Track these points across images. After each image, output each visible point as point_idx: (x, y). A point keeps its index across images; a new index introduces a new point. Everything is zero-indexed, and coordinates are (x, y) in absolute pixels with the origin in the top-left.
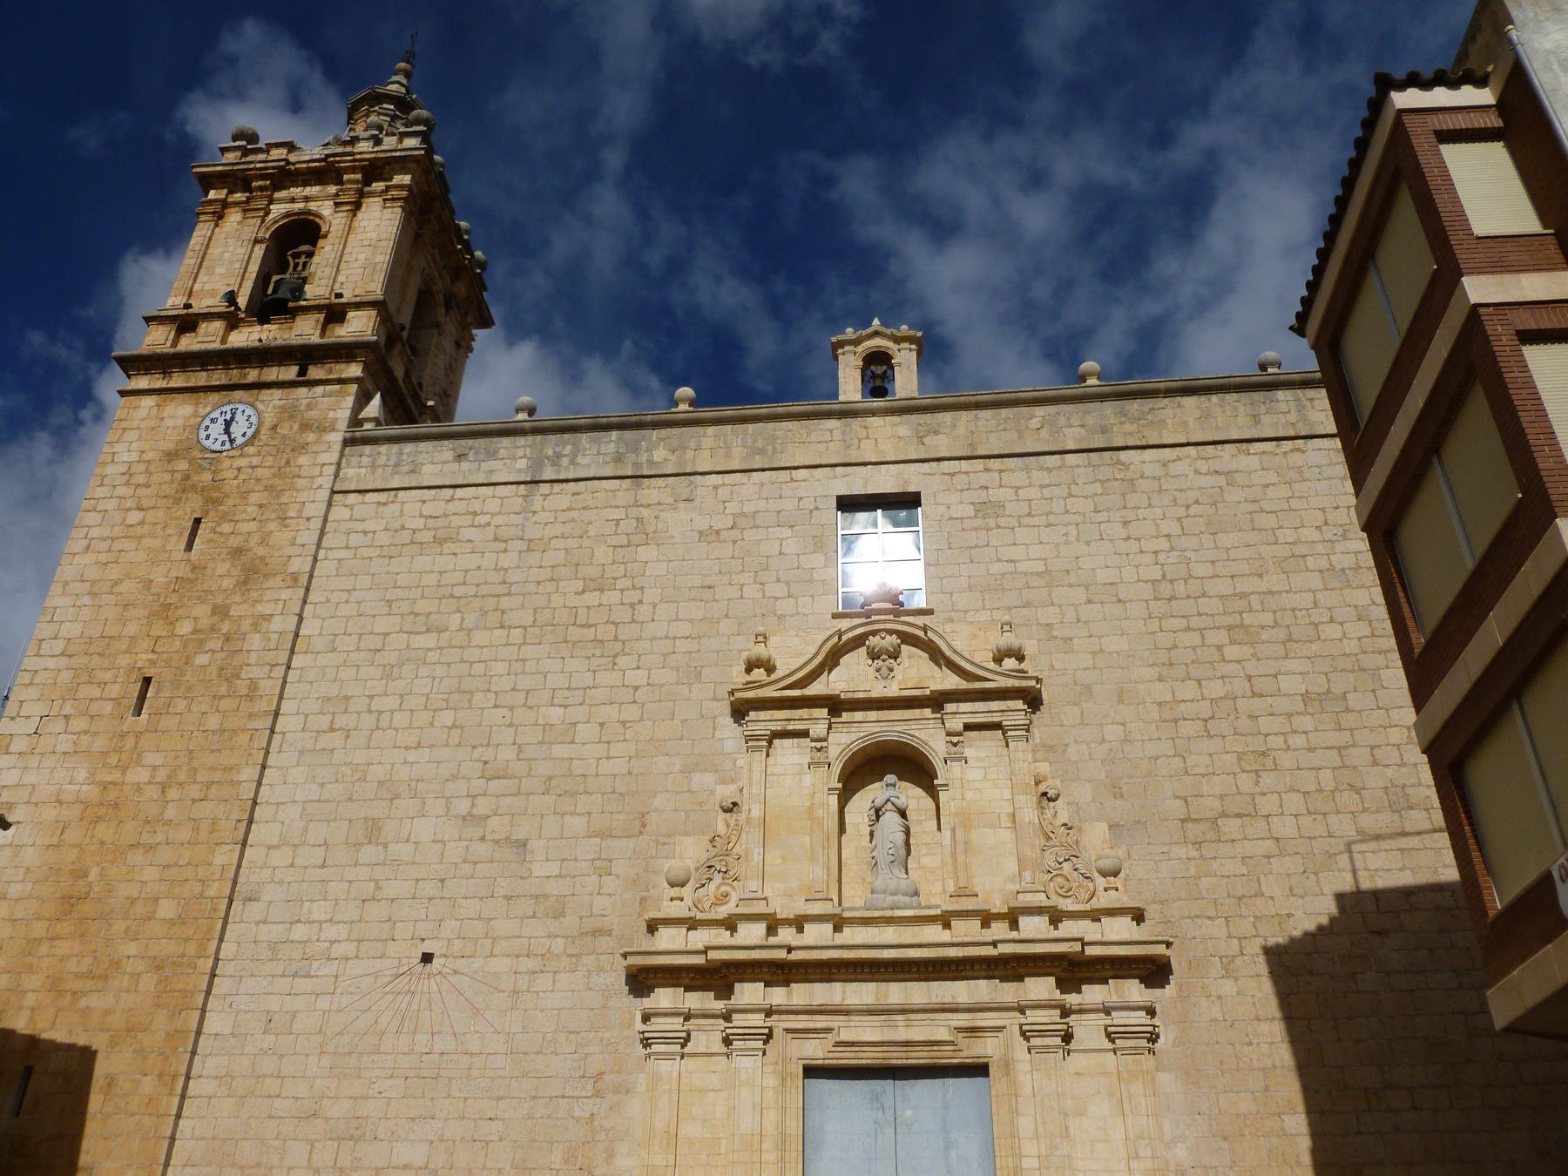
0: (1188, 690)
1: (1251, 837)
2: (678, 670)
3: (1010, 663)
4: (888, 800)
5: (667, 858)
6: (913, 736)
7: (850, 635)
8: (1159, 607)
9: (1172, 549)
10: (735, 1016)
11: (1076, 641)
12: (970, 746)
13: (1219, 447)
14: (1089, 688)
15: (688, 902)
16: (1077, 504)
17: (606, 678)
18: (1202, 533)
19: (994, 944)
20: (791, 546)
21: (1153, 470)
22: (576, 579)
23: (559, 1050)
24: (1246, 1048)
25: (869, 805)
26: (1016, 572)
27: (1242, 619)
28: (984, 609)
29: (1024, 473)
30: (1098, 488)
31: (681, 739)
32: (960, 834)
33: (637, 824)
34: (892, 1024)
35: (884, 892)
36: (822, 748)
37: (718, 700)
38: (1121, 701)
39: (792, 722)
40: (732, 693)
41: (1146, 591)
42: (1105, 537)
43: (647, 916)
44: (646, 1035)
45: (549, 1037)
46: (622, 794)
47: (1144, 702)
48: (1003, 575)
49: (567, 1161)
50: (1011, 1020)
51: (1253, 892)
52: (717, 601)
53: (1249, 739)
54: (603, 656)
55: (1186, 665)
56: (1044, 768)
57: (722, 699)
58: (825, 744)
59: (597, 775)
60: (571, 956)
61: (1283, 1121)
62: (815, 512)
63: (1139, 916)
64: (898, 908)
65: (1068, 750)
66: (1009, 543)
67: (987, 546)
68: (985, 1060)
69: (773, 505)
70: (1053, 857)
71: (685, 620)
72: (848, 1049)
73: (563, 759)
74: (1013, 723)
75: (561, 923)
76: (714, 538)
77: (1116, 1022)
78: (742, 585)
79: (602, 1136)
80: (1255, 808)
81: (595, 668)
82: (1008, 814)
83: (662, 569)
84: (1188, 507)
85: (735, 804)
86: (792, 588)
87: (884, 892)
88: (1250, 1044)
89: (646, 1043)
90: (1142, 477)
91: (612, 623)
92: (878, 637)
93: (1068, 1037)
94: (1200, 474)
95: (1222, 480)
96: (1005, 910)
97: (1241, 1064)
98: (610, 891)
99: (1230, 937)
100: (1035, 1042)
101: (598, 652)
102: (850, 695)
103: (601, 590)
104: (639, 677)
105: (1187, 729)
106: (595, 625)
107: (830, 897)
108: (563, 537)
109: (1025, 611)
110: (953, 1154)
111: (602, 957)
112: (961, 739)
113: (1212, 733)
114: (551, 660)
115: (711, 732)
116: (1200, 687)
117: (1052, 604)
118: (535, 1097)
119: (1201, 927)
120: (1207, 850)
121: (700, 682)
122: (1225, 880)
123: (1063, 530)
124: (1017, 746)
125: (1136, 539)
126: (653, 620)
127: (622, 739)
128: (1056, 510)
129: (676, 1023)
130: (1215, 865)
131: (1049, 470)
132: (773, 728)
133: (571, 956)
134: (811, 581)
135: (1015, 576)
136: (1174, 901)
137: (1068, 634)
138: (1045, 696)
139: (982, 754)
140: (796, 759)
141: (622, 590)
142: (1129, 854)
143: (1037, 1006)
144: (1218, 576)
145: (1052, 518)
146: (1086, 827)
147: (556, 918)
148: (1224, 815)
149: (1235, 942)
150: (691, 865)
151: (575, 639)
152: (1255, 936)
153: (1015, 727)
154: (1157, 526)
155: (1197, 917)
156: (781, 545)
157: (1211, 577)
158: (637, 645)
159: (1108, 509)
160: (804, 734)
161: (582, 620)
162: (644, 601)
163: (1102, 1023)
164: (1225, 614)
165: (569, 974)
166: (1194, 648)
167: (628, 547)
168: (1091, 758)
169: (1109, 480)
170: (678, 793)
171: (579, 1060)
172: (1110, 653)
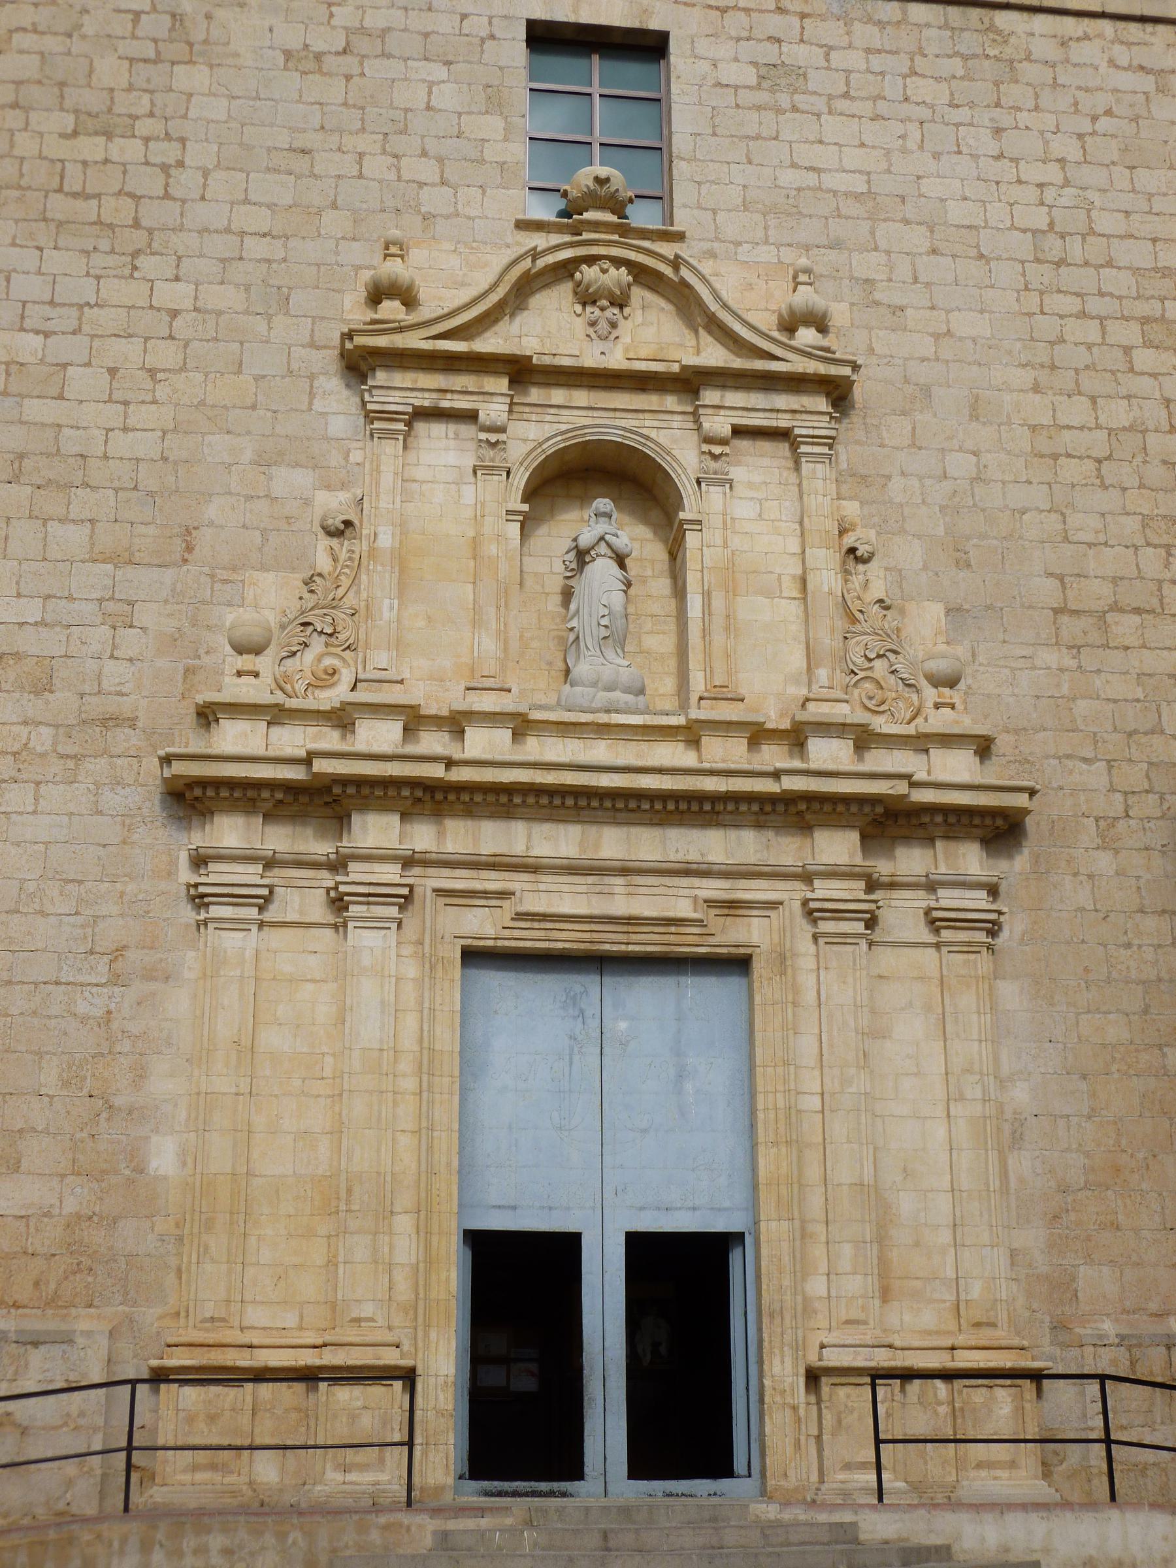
0: (1076, 411)
1: (1152, 645)
2: (248, 288)
3: (807, 336)
4: (602, 538)
5: (230, 604)
6: (648, 438)
7: (550, 259)
8: (1040, 275)
9: (1067, 183)
10: (352, 866)
11: (909, 312)
12: (739, 463)
13: (1149, 28)
14: (927, 391)
15: (267, 678)
16: (921, 89)
17: (117, 290)
18: (1113, 163)
19: (776, 775)
20: (447, 97)
21: (1044, 49)
22: (62, 109)
23: (49, 908)
24: (1122, 951)
25: (569, 544)
26: (820, 189)
27: (1164, 310)
28: (766, 242)
29: (841, 23)
30: (956, 66)
31: (254, 407)
32: (718, 602)
33: (178, 545)
34: (606, 889)
35: (594, 684)
36: (498, 442)
37: (318, 348)
38: (974, 417)
39: (449, 396)
40: (349, 335)
41: (1022, 245)
42: (964, 149)
43: (200, 699)
44: (202, 889)
45: (31, 886)
46: (150, 494)
47: (1009, 423)
48: (799, 190)
49: (66, 1084)
50: (791, 894)
51: (1148, 726)
52: (316, 177)
53: (1161, 496)
54: (112, 251)
55: (1076, 370)
56: (851, 509)
57: (325, 347)
58: (502, 437)
59: (106, 457)
60: (62, 756)
61: (1164, 1055)
62: (489, 43)
63: (984, 748)
64: (617, 711)
65: (890, 485)
66: (811, 138)
67: (776, 138)
68: (748, 951)
69: (417, 22)
70: (860, 650)
71: (260, 204)
72: (536, 925)
73: (43, 425)
74: (811, 432)
75: (47, 702)
76: (311, 65)
77: (943, 903)
78: (361, 155)
79: (126, 1046)
80: (1161, 600)
81: (98, 272)
82: (794, 577)
83: (218, 109)
84: (1095, 119)
85: (348, 524)
86: (447, 170)
87: (594, 684)
88: (1128, 945)
89: (199, 900)
90: (1028, 58)
91: (131, 195)
92: (596, 268)
93: (871, 923)
94: (1117, 67)
95: (1148, 83)
96: (785, 724)
97: (1115, 975)
98: (130, 654)
99: (1112, 790)
100: (826, 927)
101: (104, 245)
102: (547, 360)
103: (109, 135)
104: (177, 295)
105: (1071, 470)
106: (98, 196)
107: (507, 686)
108: (35, 31)
109: (833, 255)
110: (689, 1087)
111: (119, 762)
112: (727, 450)
113: (1108, 482)
114: (18, 249)
115: (305, 399)
116: (1095, 409)
117: (876, 249)
118: (9, 982)
119: (1071, 772)
120: (1089, 659)
121: (287, 313)
122: (1111, 705)
123: (899, 129)
124: (817, 474)
125: (1011, 160)
126: (203, 198)
127: (149, 398)
128: (887, 93)
129: (250, 874)
130: (1098, 682)
131: (882, 25)
132: (417, 403)
133: (62, 756)
134: (482, 161)
135: (819, 194)
136: (1036, 732)
137: (898, 301)
138: (857, 393)
139: (757, 478)
140: (452, 458)
141: (147, 140)
142: (974, 655)
143: (833, 873)
144: (1132, 236)
145: (882, 107)
146: (911, 607)
147: (37, 693)
148: (1116, 607)
149: (1119, 797)
150: (272, 618)
151: (59, 216)
152: (1147, 792)
153: (814, 439)
154: (1046, 143)
155: (1068, 757)
156: (430, 93)
157: (1121, 237)
158: (174, 238)
159: (972, 105)
160: (471, 416)
161: (73, 183)
162: (188, 162)
163: (924, 904)
164: (1138, 297)
165: (62, 787)
166: (1089, 347)
167: (155, 62)
168: (924, 502)
169: (975, 56)
170: (249, 498)
171: (83, 926)
172: (961, 339)
